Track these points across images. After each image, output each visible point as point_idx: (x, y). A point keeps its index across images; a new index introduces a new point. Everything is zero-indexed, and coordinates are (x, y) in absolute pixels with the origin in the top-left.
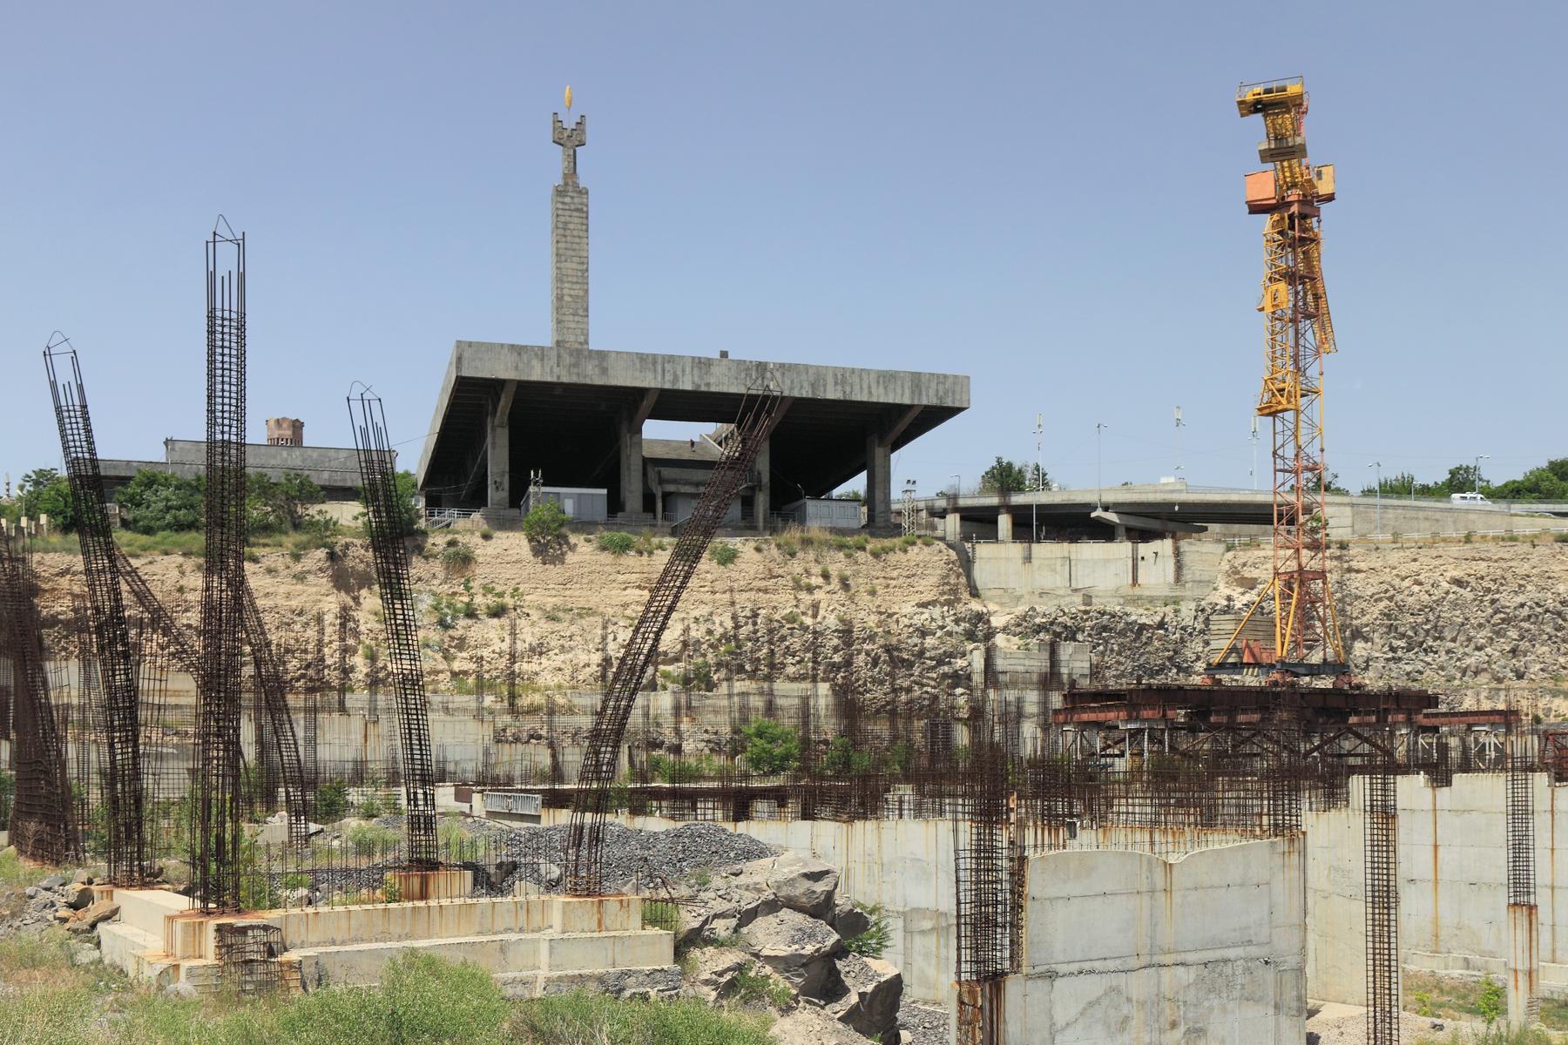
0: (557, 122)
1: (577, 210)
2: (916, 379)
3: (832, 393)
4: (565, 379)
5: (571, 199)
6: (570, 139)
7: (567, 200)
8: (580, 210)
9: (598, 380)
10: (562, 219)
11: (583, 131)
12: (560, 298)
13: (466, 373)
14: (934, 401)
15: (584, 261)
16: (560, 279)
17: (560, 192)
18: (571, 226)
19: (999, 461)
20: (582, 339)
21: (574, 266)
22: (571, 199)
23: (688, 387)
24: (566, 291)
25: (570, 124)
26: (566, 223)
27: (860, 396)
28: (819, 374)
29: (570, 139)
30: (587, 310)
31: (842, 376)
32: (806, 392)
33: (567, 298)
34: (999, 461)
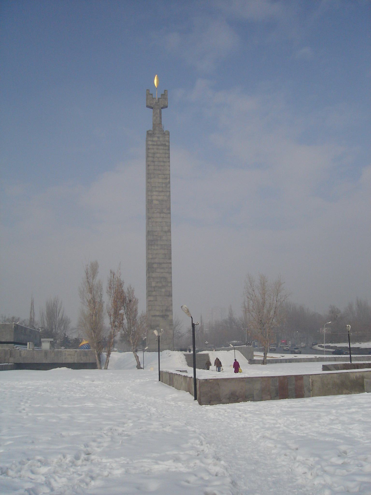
1: (162, 145)
7: (155, 139)
8: (165, 145)
10: (152, 151)
11: (166, 99)
12: (149, 202)
15: (167, 177)
16: (149, 190)
17: (150, 134)
18: (158, 155)
20: (166, 229)
21: (160, 181)
24: (154, 197)
26: (154, 153)
30: (169, 209)
33: (155, 202)
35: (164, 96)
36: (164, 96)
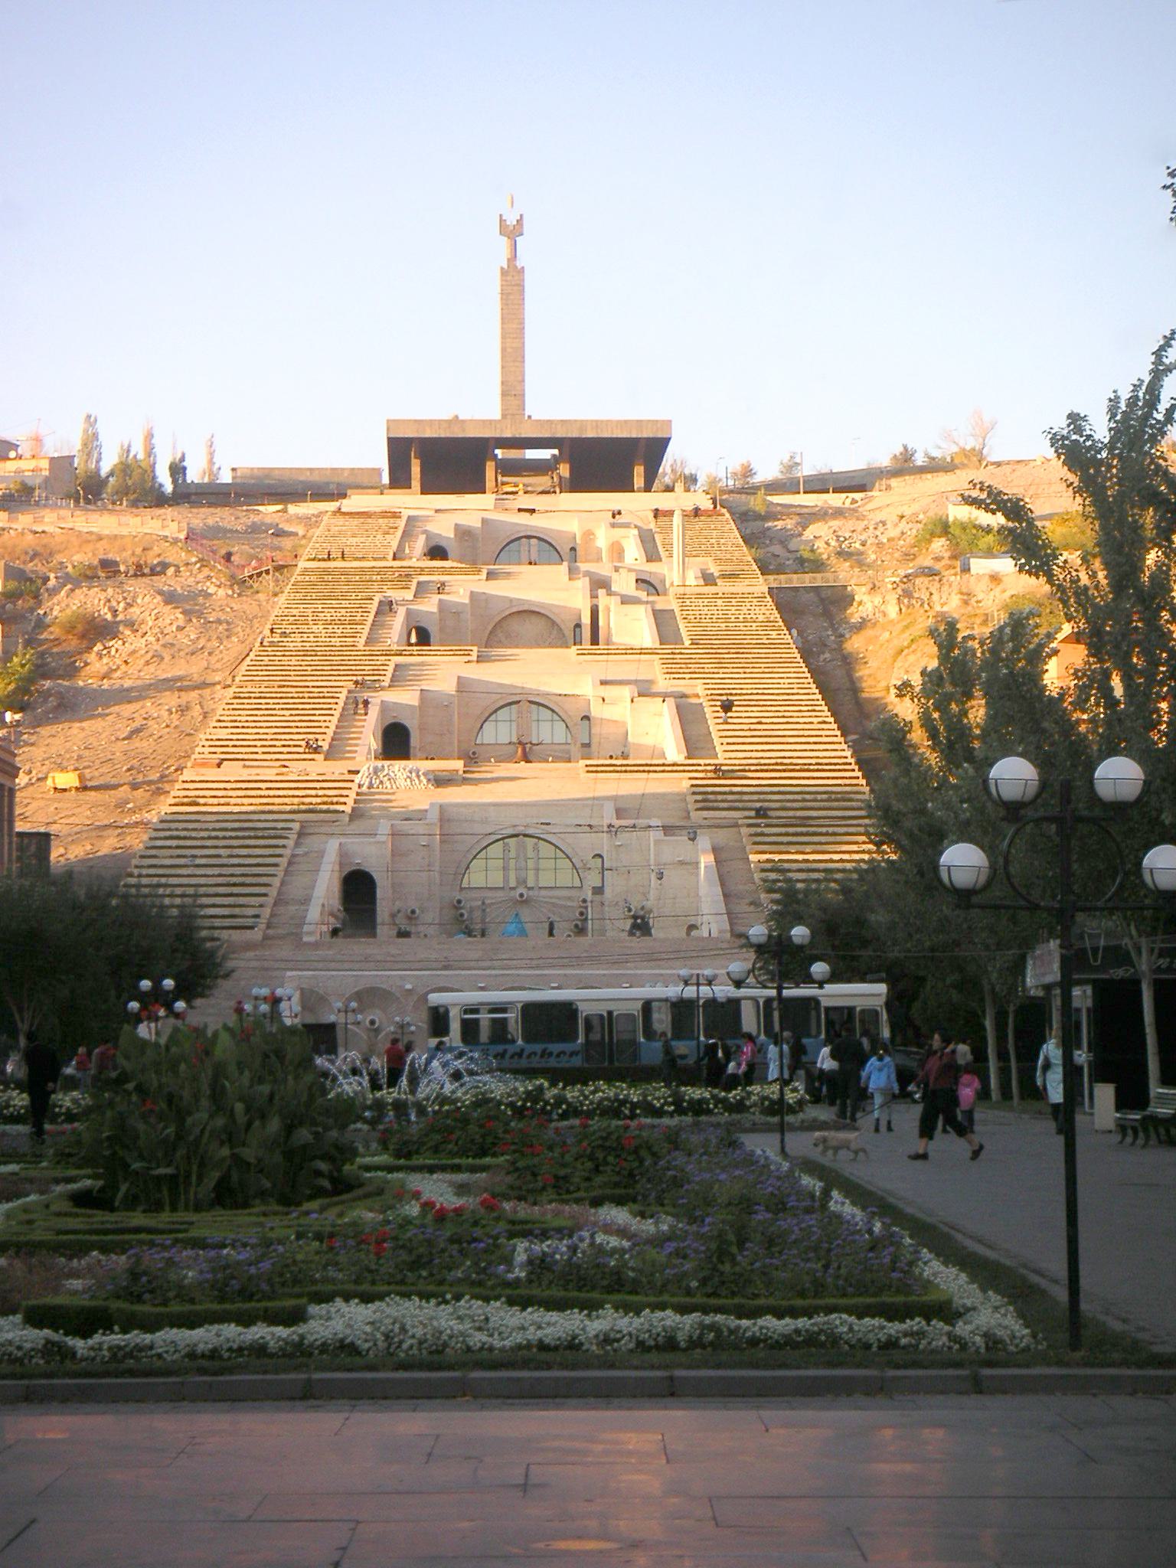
0: (502, 220)
2: (640, 423)
3: (590, 434)
4: (443, 436)
5: (513, 281)
6: (512, 232)
9: (460, 436)
12: (504, 350)
13: (392, 435)
14: (651, 435)
16: (503, 337)
17: (504, 272)
19: (905, 448)
22: (513, 281)
23: (509, 435)
25: (511, 220)
27: (606, 434)
28: (583, 424)
29: (512, 232)
31: (597, 424)
32: (575, 435)
34: (905, 448)
35: (520, 221)
36: (520, 221)
